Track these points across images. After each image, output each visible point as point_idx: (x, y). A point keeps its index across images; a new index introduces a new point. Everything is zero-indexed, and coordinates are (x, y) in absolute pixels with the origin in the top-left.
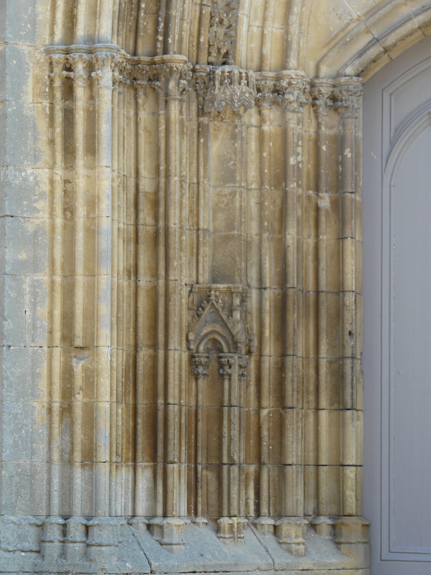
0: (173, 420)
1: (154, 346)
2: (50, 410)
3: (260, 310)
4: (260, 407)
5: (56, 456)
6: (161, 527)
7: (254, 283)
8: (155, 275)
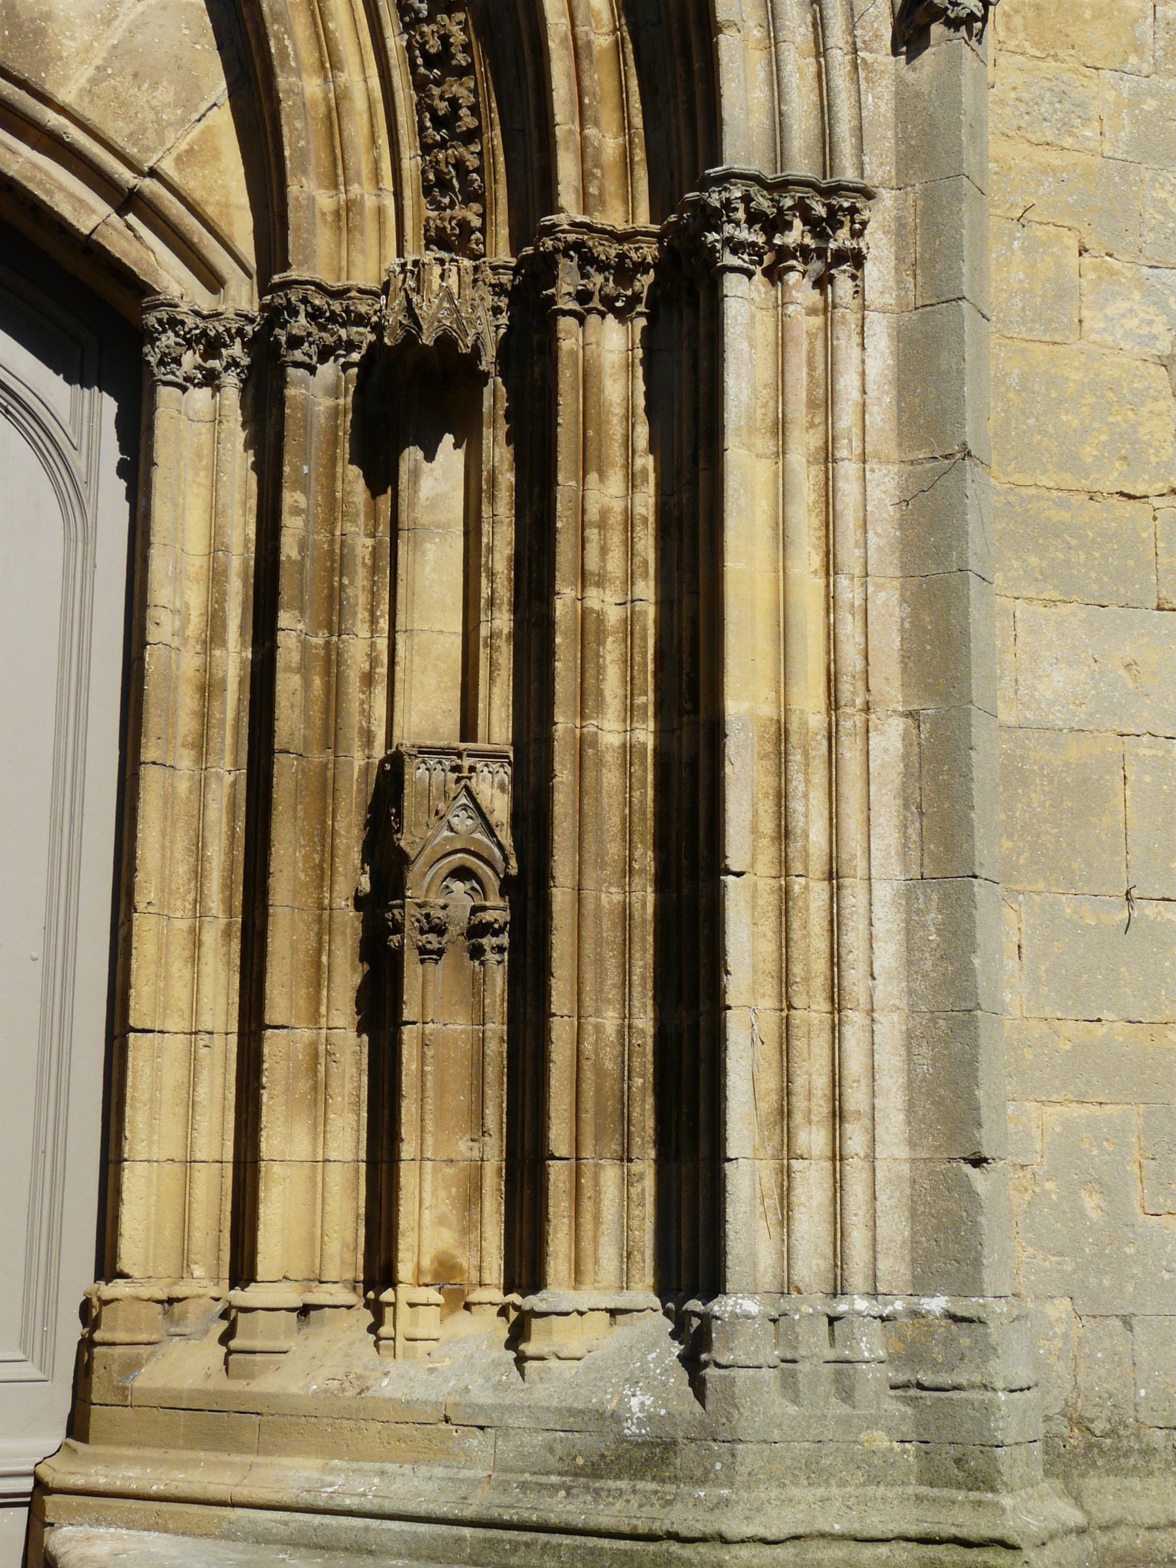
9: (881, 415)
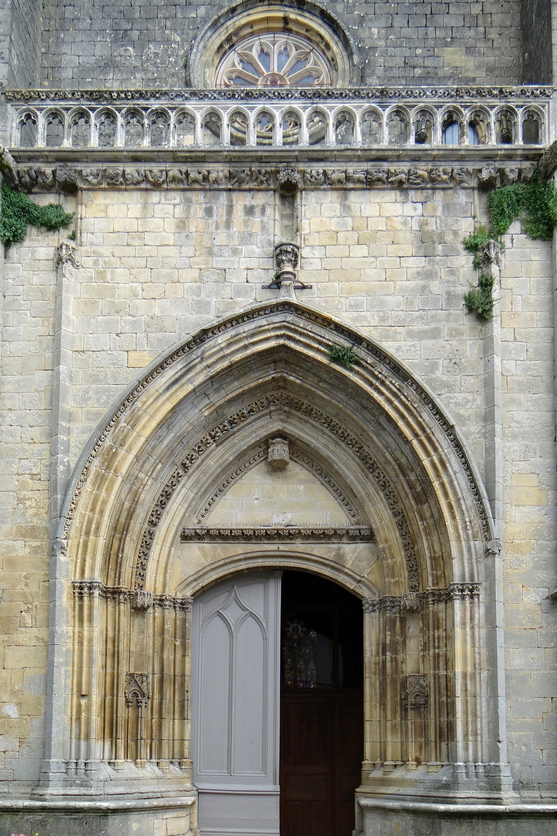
0: (119, 723)
1: (112, 695)
2: (71, 719)
3: (153, 682)
4: (152, 718)
5: (73, 736)
6: (114, 763)
7: (151, 672)
8: (113, 668)
9: (482, 621)
